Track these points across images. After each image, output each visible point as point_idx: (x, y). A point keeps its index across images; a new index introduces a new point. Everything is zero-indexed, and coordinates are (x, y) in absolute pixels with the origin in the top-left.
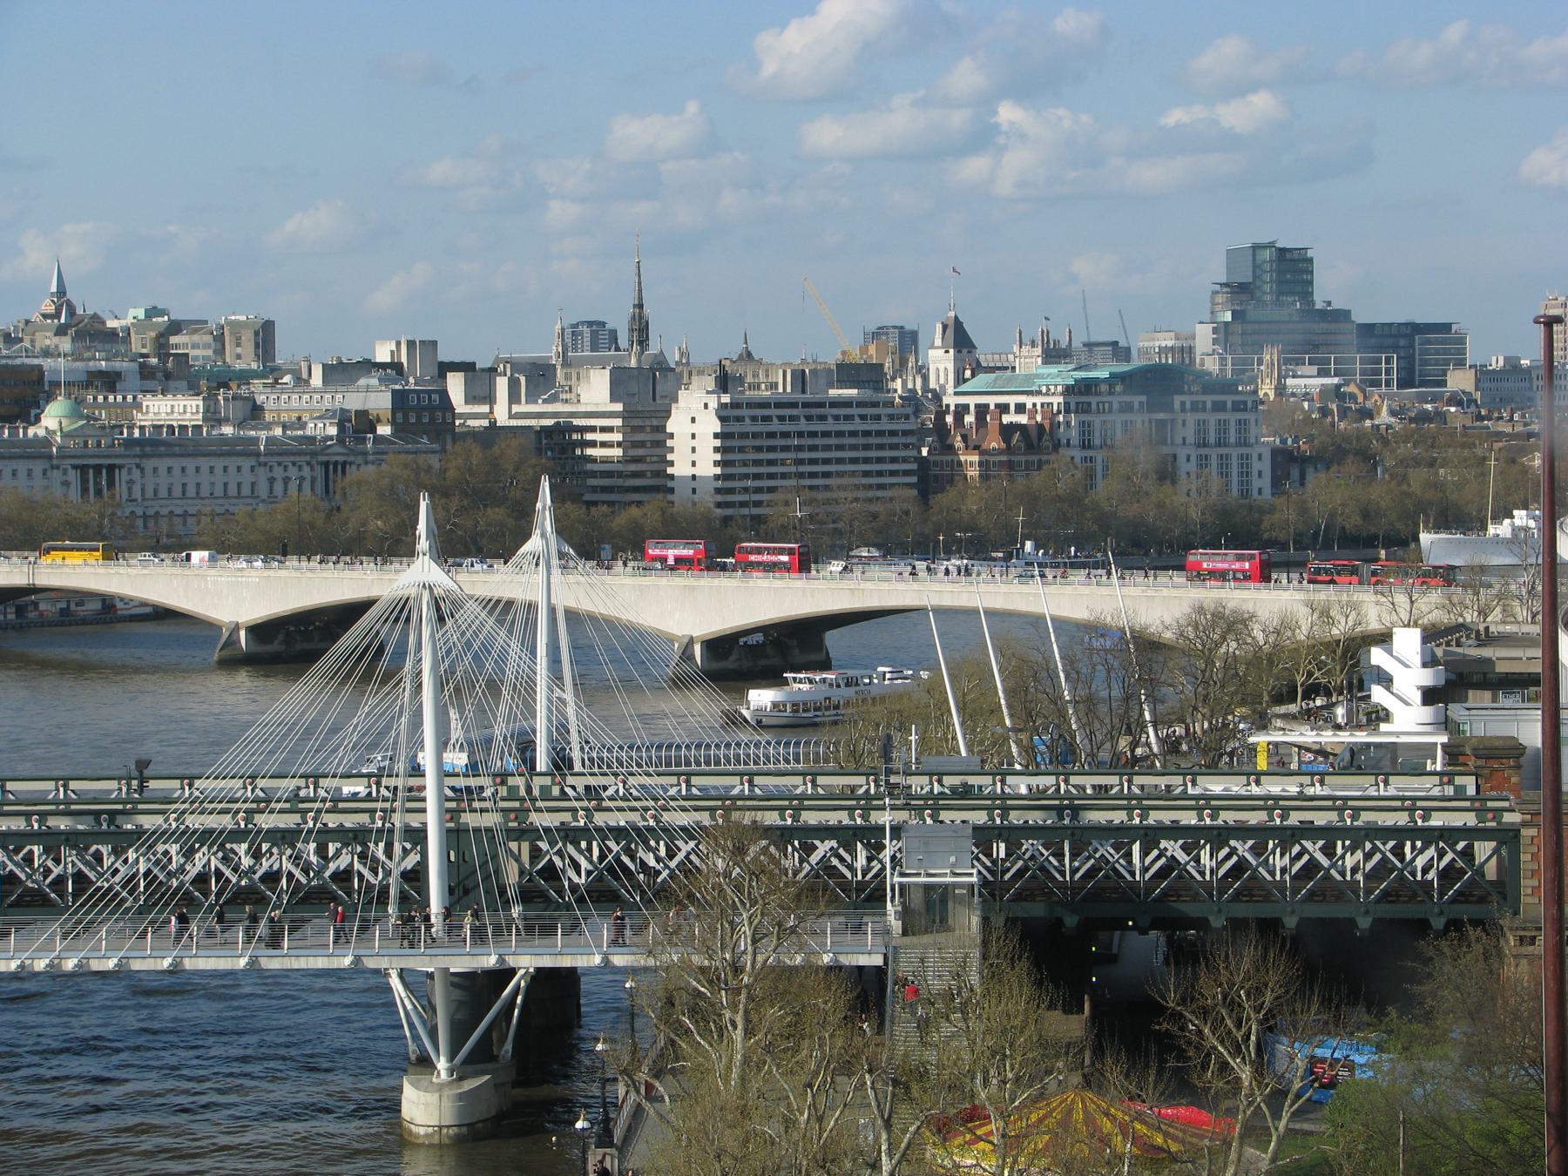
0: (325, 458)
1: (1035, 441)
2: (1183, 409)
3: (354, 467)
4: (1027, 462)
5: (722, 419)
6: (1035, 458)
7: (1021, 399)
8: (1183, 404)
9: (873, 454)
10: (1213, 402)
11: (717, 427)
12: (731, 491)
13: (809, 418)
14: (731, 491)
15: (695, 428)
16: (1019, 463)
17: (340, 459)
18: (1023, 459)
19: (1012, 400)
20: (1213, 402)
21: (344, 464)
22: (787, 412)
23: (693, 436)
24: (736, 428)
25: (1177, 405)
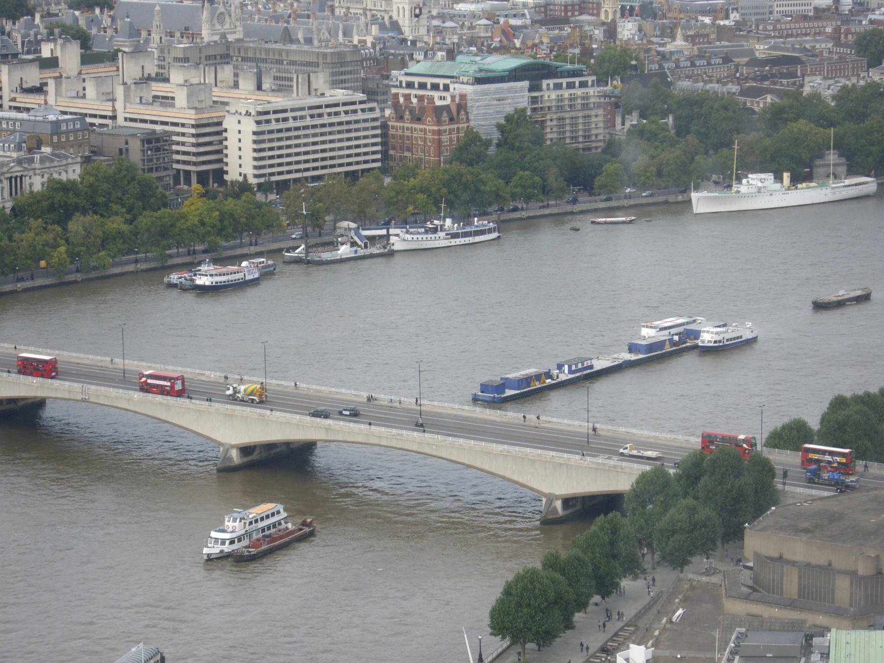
0: (9, 175)
1: (455, 115)
2: (548, 89)
3: (27, 178)
4: (450, 130)
5: (258, 123)
6: (455, 126)
7: (447, 81)
8: (548, 85)
9: (353, 135)
10: (567, 83)
11: (254, 128)
12: (263, 167)
13: (312, 116)
14: (263, 167)
15: (240, 127)
16: (445, 131)
17: (19, 174)
18: (447, 127)
19: (441, 82)
20: (567, 83)
21: (21, 177)
22: (298, 114)
23: (240, 132)
24: (265, 127)
25: (544, 86)
